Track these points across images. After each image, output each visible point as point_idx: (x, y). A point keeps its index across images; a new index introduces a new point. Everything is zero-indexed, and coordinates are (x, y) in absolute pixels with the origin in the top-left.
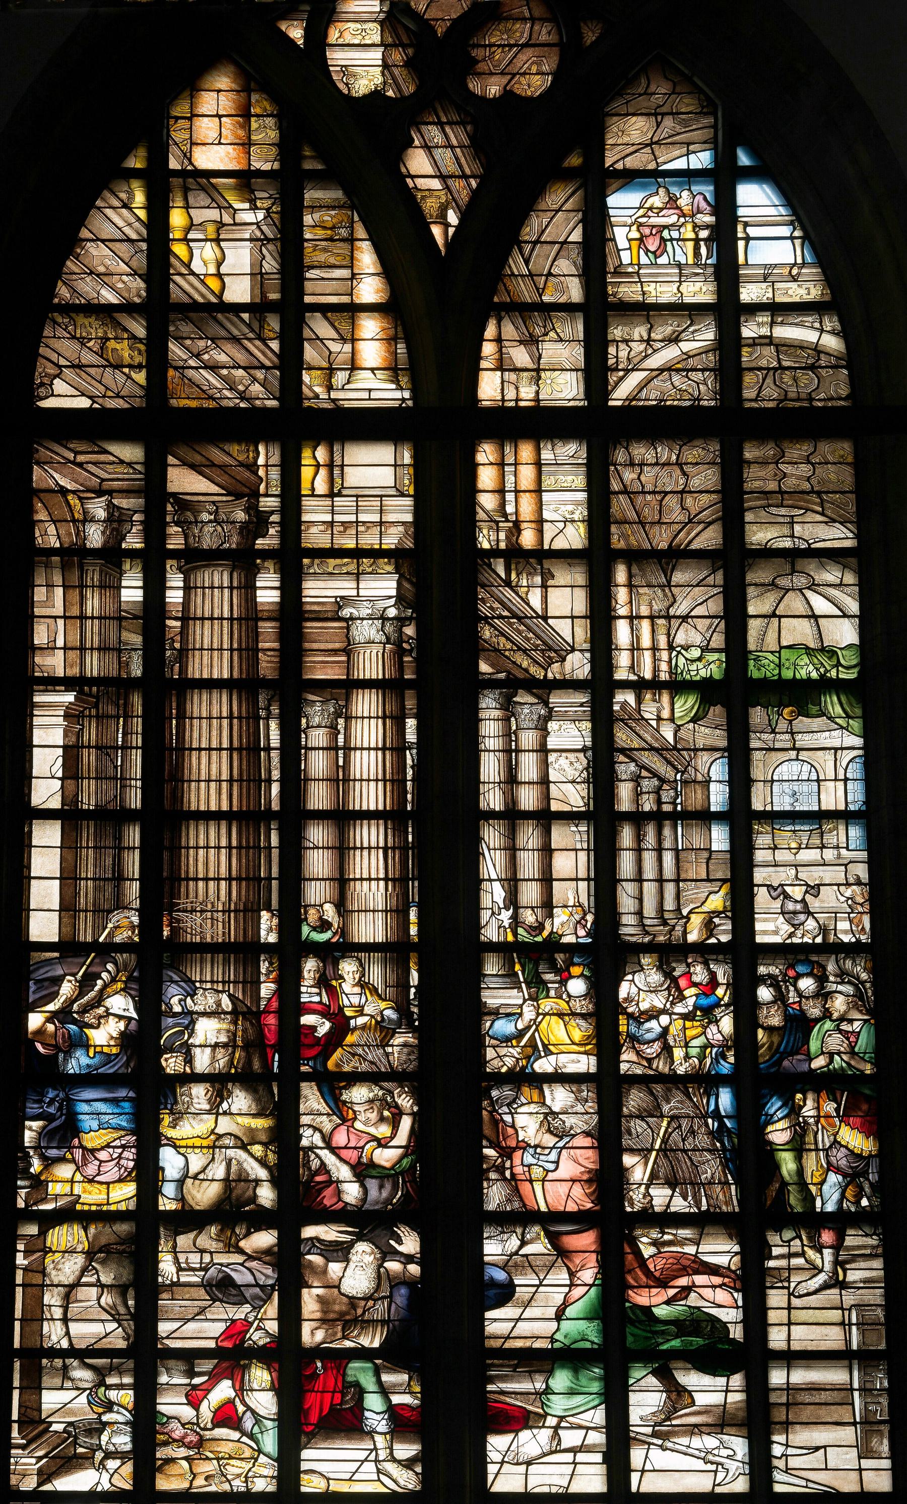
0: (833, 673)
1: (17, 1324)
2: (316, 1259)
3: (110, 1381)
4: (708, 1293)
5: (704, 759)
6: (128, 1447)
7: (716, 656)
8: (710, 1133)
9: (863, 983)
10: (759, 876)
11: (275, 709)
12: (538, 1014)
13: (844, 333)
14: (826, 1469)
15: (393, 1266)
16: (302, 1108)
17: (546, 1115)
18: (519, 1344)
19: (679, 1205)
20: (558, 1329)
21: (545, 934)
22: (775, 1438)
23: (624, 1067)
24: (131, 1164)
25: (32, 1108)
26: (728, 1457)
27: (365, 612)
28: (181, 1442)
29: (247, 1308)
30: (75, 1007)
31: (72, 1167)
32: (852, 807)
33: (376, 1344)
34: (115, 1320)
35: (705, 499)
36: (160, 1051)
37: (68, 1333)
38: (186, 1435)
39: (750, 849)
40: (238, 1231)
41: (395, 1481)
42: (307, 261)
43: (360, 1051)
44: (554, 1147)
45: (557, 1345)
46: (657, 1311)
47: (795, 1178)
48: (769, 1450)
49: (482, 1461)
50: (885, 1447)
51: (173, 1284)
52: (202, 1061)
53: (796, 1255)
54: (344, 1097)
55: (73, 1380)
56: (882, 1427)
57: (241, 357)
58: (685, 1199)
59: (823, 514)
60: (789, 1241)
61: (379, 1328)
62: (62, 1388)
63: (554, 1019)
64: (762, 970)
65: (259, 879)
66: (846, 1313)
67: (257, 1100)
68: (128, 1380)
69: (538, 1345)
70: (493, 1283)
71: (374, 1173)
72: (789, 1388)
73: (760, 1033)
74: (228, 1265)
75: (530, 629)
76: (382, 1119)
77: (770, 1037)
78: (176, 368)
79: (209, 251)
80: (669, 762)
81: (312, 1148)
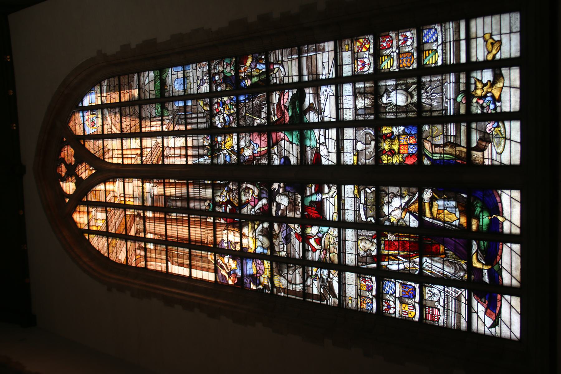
0: (159, 77)
1: (297, 298)
2: (280, 212)
3: (310, 274)
4: (285, 100)
5: (175, 107)
6: (327, 270)
7: (157, 106)
8: (249, 102)
9: (216, 63)
10: (196, 92)
11: (170, 214)
12: (225, 149)
13: (104, 80)
14: (328, 61)
15: (281, 191)
16: (246, 214)
17: (246, 147)
18: (299, 155)
19: (265, 110)
20: (295, 143)
21: (209, 147)
22: (321, 78)
23: (235, 126)
24: (260, 261)
25: (248, 285)
26: (326, 92)
27: (152, 191)
28: (325, 255)
29: (292, 233)
30: (227, 271)
31: (261, 277)
32: (182, 69)
33: (300, 196)
34: (296, 270)
35: (131, 110)
36: (236, 250)
37: (299, 284)
38: (323, 253)
39: (191, 94)
40: (274, 234)
41: (334, 193)
42: (99, 201)
43: (234, 197)
44: (253, 145)
45: (299, 144)
46: (290, 116)
47: (258, 77)
48: (324, 79)
49: (328, 166)
50: (322, 44)
51: (287, 253)
52: (238, 239)
53: (276, 75)
54: (244, 202)
55: (310, 285)
56: (317, 46)
57: (114, 216)
58: (264, 108)
59: (132, 82)
60: (273, 78)
61: (296, 195)
62: (312, 288)
63: (226, 145)
64: (214, 90)
65: (201, 221)
66: (289, 60)
67: (245, 226)
68: (310, 269)
69: (299, 150)
70: (284, 162)
71: (260, 195)
72: (308, 75)
73: (227, 89)
74: (282, 237)
75: (154, 152)
76: (248, 192)
77: (228, 87)
78: (116, 231)
79: (99, 221)
80: (175, 117)
81: (255, 211)
